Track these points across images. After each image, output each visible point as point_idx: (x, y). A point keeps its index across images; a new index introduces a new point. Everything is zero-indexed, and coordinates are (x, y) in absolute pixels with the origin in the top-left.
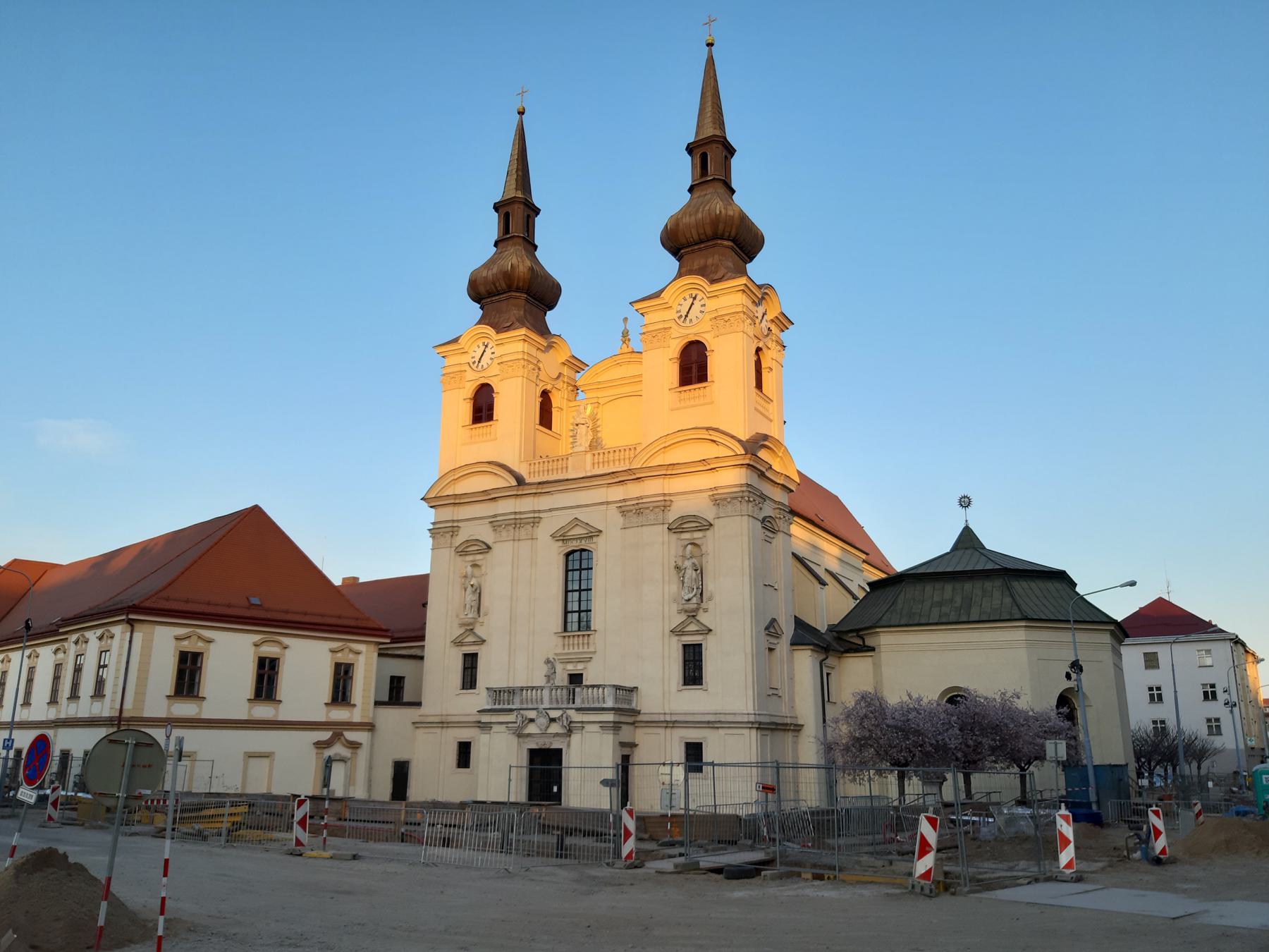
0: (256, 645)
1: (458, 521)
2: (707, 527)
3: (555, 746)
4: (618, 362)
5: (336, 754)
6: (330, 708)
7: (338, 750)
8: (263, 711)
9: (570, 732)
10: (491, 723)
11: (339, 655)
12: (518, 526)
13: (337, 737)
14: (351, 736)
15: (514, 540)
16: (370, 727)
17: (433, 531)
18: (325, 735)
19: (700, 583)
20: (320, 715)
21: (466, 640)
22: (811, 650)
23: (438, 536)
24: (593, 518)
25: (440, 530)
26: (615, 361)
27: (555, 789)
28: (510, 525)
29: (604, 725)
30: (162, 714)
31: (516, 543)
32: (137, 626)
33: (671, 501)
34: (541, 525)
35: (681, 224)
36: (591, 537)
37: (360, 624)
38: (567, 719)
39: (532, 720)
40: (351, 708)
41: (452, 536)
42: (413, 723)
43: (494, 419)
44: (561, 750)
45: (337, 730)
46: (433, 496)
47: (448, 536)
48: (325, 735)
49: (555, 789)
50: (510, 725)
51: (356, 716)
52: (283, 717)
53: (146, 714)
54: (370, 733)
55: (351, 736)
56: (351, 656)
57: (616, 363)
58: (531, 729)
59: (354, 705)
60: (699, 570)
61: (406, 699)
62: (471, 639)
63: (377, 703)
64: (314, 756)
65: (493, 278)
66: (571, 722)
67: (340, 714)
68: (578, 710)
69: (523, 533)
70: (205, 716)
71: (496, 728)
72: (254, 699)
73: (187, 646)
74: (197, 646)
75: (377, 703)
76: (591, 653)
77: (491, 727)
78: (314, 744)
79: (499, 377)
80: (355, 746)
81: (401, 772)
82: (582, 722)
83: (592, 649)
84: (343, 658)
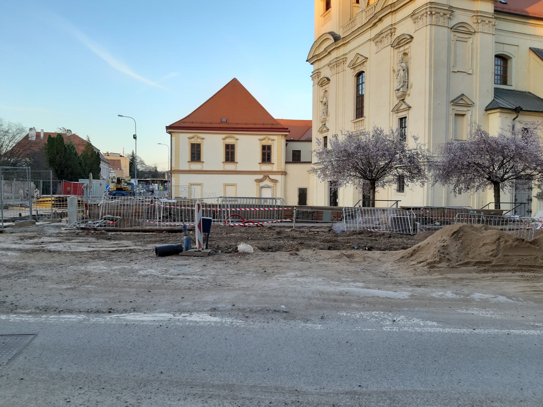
0: (224, 139)
2: (410, 40)
5: (265, 185)
6: (261, 165)
7: (267, 182)
8: (230, 167)
11: (264, 141)
12: (338, 65)
13: (266, 177)
14: (272, 177)
15: (336, 74)
16: (284, 173)
17: (312, 76)
18: (260, 177)
19: (407, 78)
20: (257, 168)
22: (500, 112)
24: (364, 51)
30: (187, 168)
32: (173, 134)
33: (395, 28)
37: (274, 126)
40: (272, 165)
45: (266, 175)
48: (260, 177)
51: (275, 168)
52: (239, 169)
53: (181, 169)
54: (283, 176)
55: (272, 177)
56: (270, 142)
59: (274, 164)
60: (407, 70)
61: (301, 161)
63: (287, 162)
64: (256, 186)
67: (266, 167)
70: (204, 169)
72: (225, 162)
73: (194, 141)
74: (198, 141)
75: (287, 162)
78: (255, 180)
80: (275, 181)
81: (303, 194)
84: (266, 143)
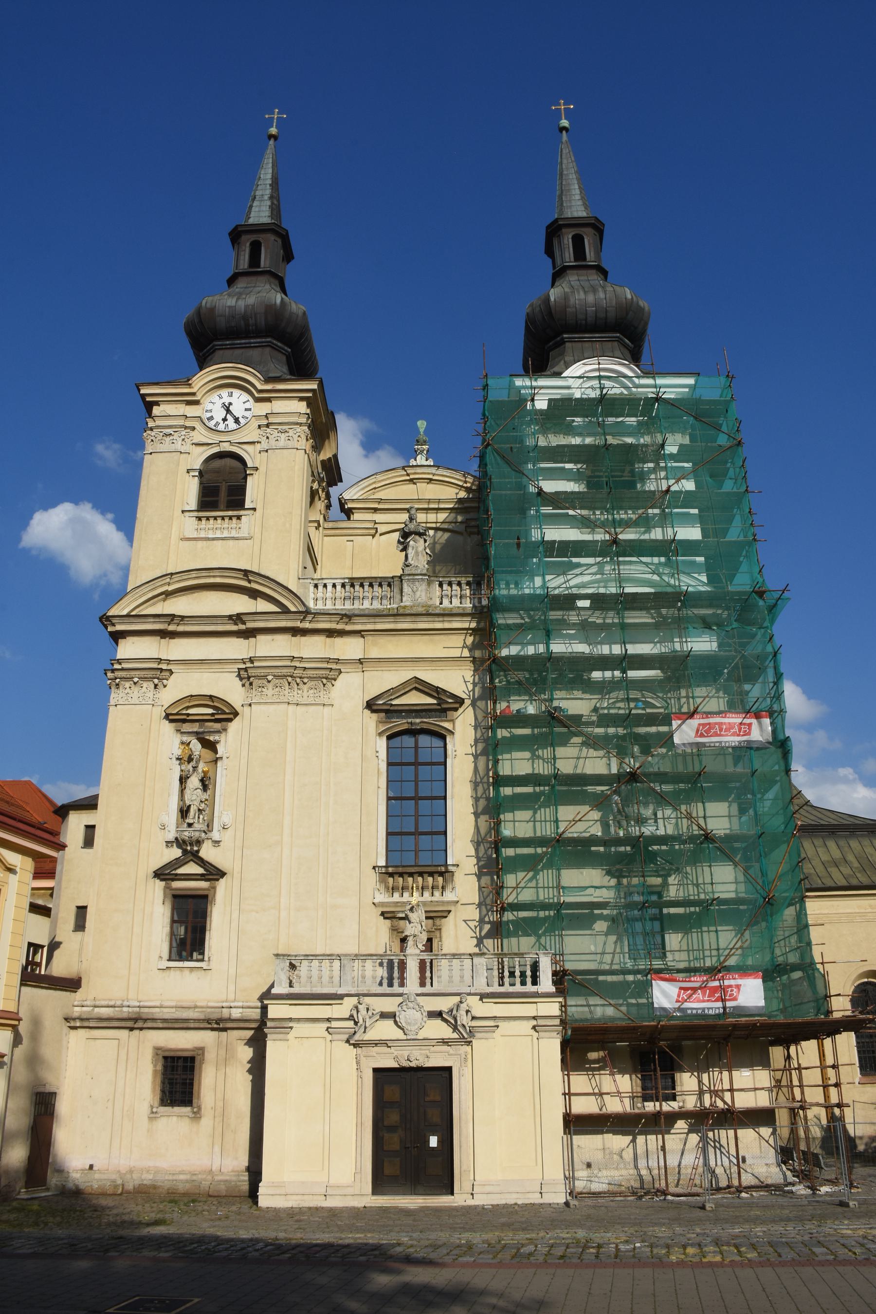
1: (169, 662)
3: (437, 1059)
4: (412, 477)
9: (466, 1037)
10: (290, 1020)
21: (181, 871)
23: (127, 685)
25: (133, 673)
26: (408, 475)
27: (433, 1141)
28: (285, 676)
29: (538, 1025)
31: (291, 708)
34: (337, 683)
35: (572, 301)
36: (445, 711)
38: (467, 1012)
39: (391, 1016)
41: (156, 686)
42: (67, 1019)
43: (248, 504)
44: (449, 1069)
46: (125, 612)
47: (148, 686)
49: (433, 1141)
50: (334, 1024)
57: (408, 478)
58: (385, 1030)
62: (192, 868)
65: (245, 311)
66: (473, 1018)
68: (483, 996)
69: (306, 693)
71: (299, 1029)
76: (449, 903)
77: (291, 1028)
79: (258, 447)
82: (494, 1018)
83: (449, 896)
